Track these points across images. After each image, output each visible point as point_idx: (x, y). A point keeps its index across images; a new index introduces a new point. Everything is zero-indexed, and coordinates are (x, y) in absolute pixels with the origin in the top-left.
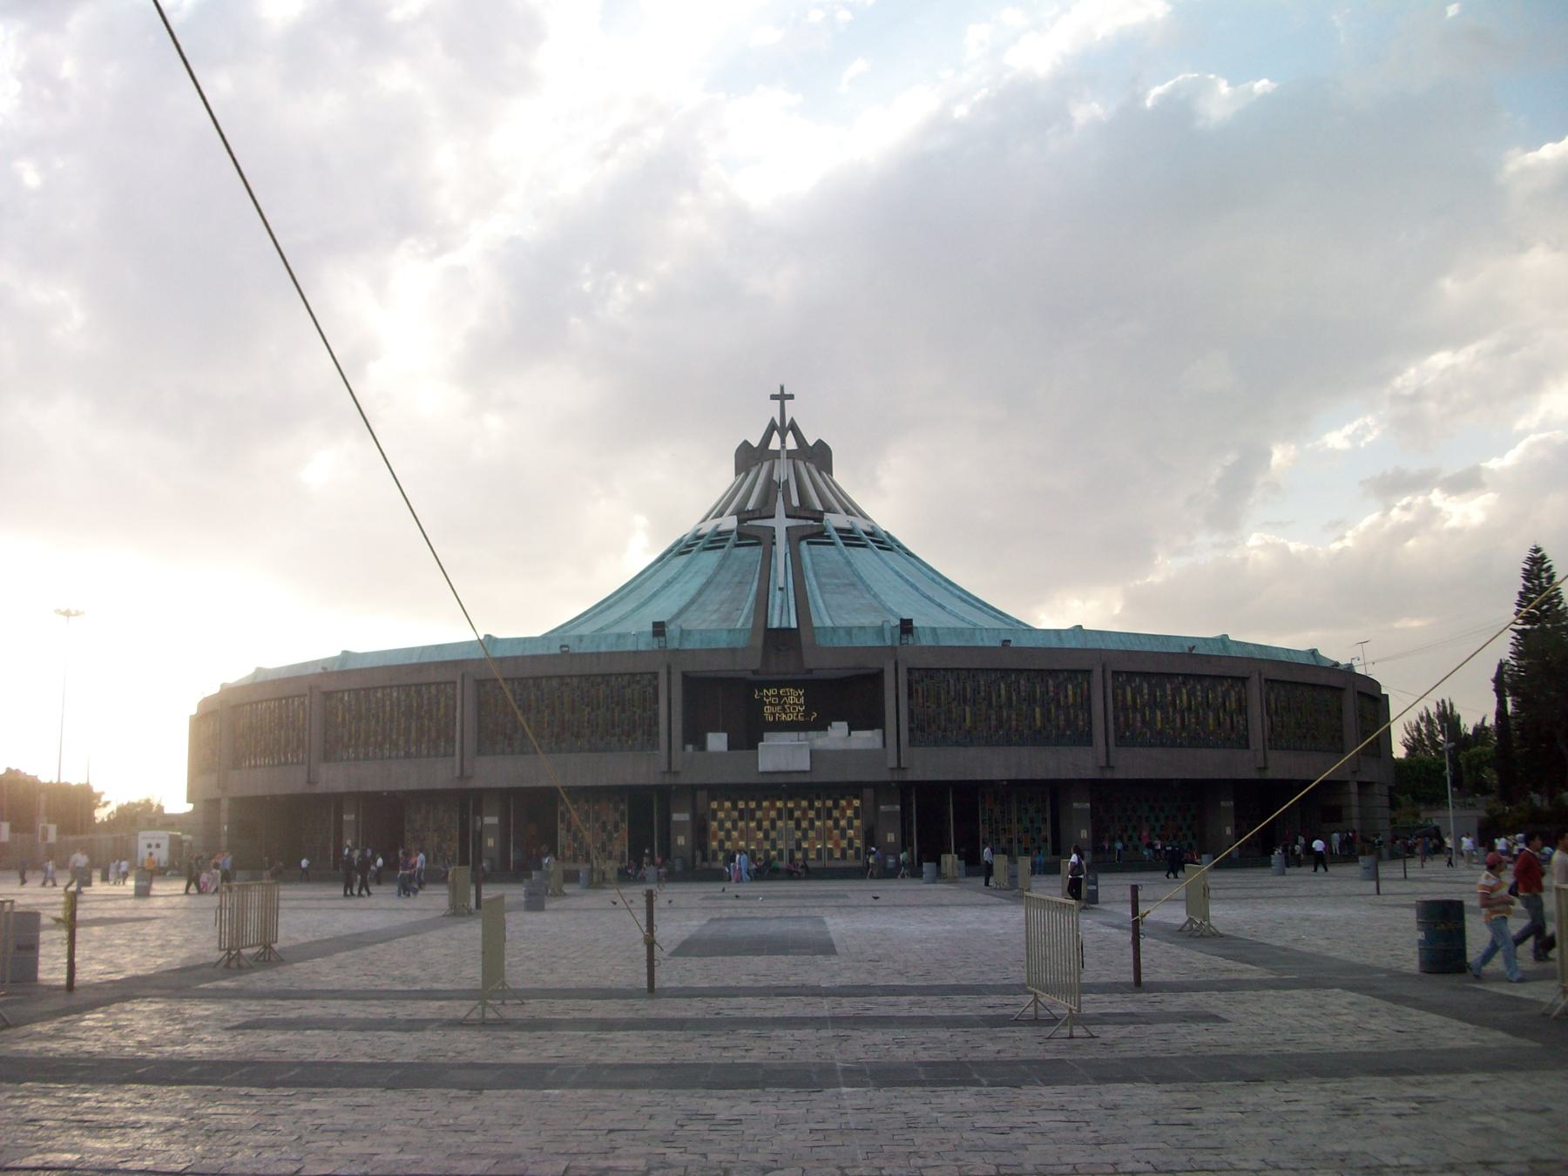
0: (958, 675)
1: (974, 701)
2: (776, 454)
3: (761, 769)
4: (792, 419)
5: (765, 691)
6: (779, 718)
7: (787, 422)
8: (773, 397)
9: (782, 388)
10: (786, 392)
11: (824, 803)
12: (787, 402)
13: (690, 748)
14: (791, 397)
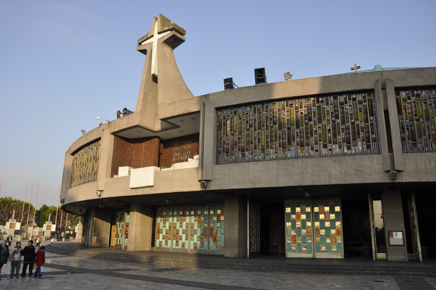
0: (255, 108)
1: (267, 126)
3: (131, 186)
5: (174, 143)
6: (179, 159)
11: (209, 212)
13: (115, 176)
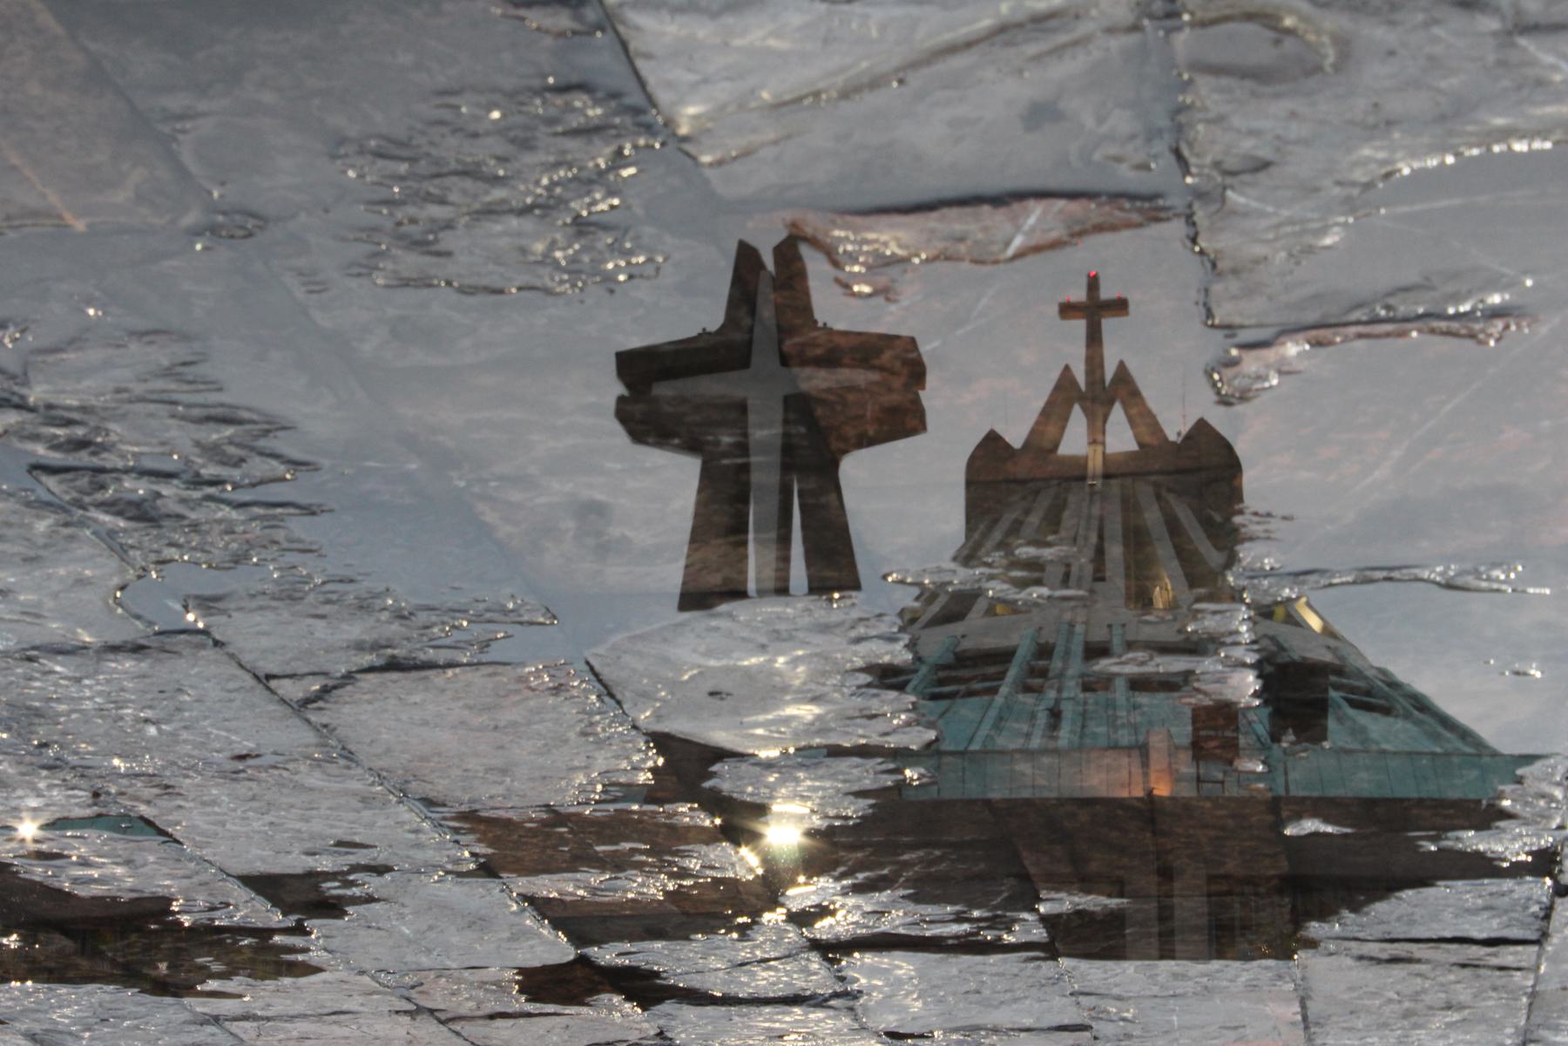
2: (1075, 473)
4: (1122, 366)
7: (1110, 371)
8: (1067, 310)
9: (1093, 283)
10: (1107, 293)
12: (1109, 324)
14: (1120, 306)
